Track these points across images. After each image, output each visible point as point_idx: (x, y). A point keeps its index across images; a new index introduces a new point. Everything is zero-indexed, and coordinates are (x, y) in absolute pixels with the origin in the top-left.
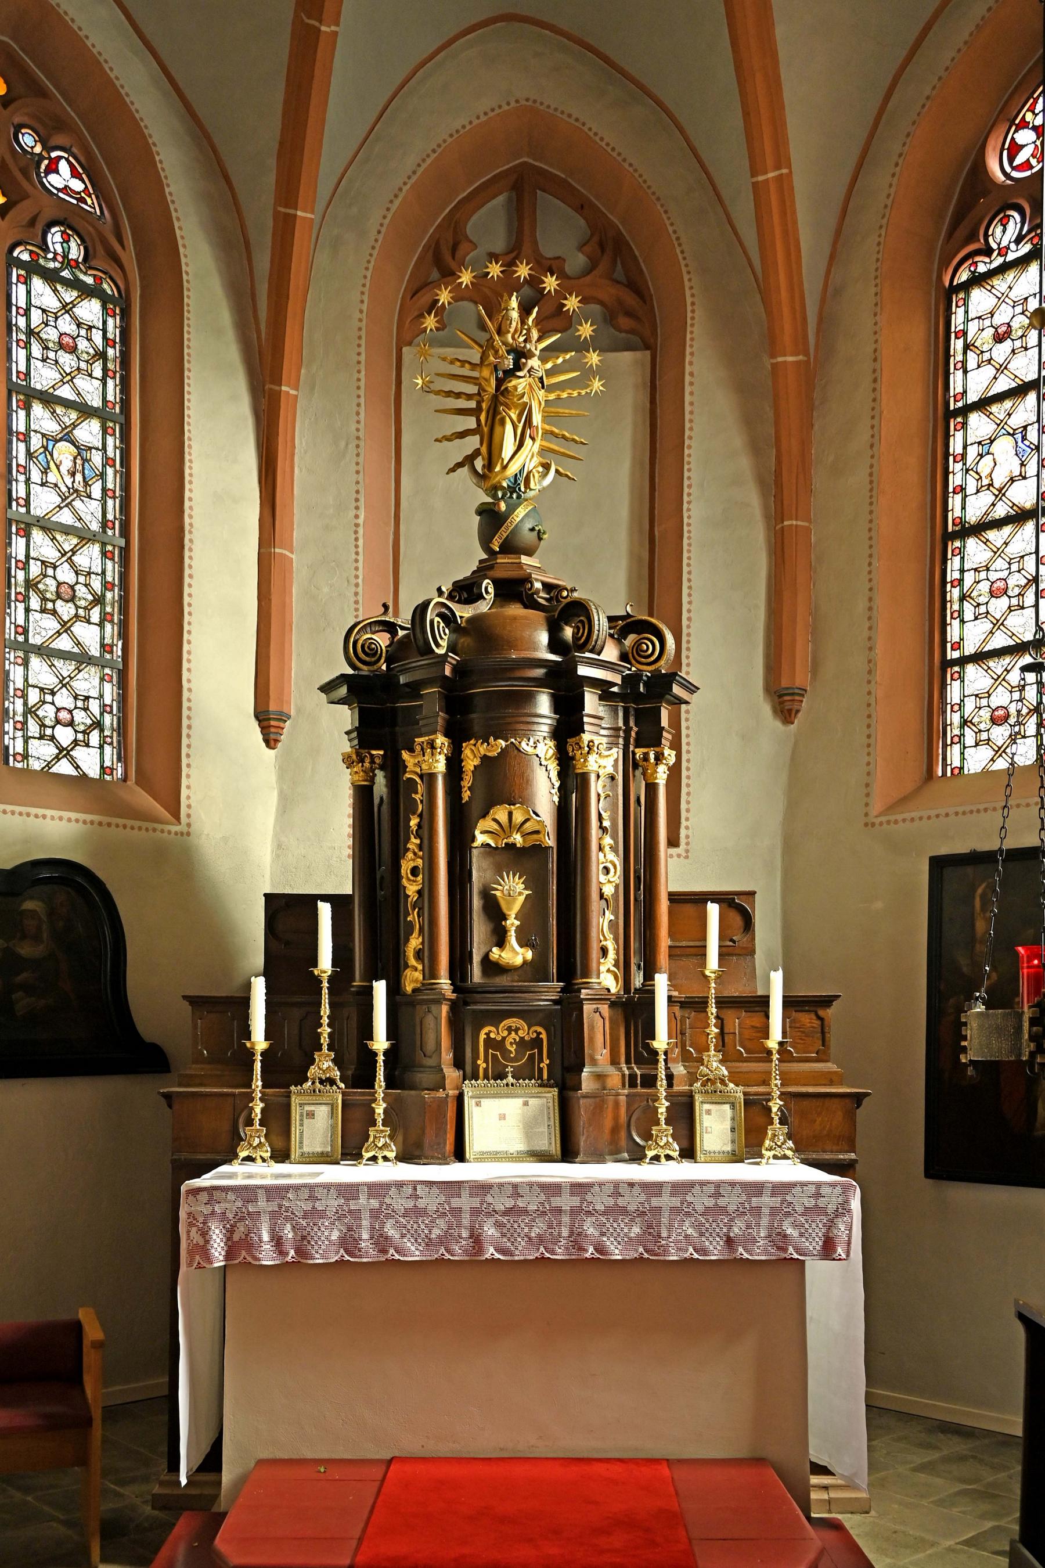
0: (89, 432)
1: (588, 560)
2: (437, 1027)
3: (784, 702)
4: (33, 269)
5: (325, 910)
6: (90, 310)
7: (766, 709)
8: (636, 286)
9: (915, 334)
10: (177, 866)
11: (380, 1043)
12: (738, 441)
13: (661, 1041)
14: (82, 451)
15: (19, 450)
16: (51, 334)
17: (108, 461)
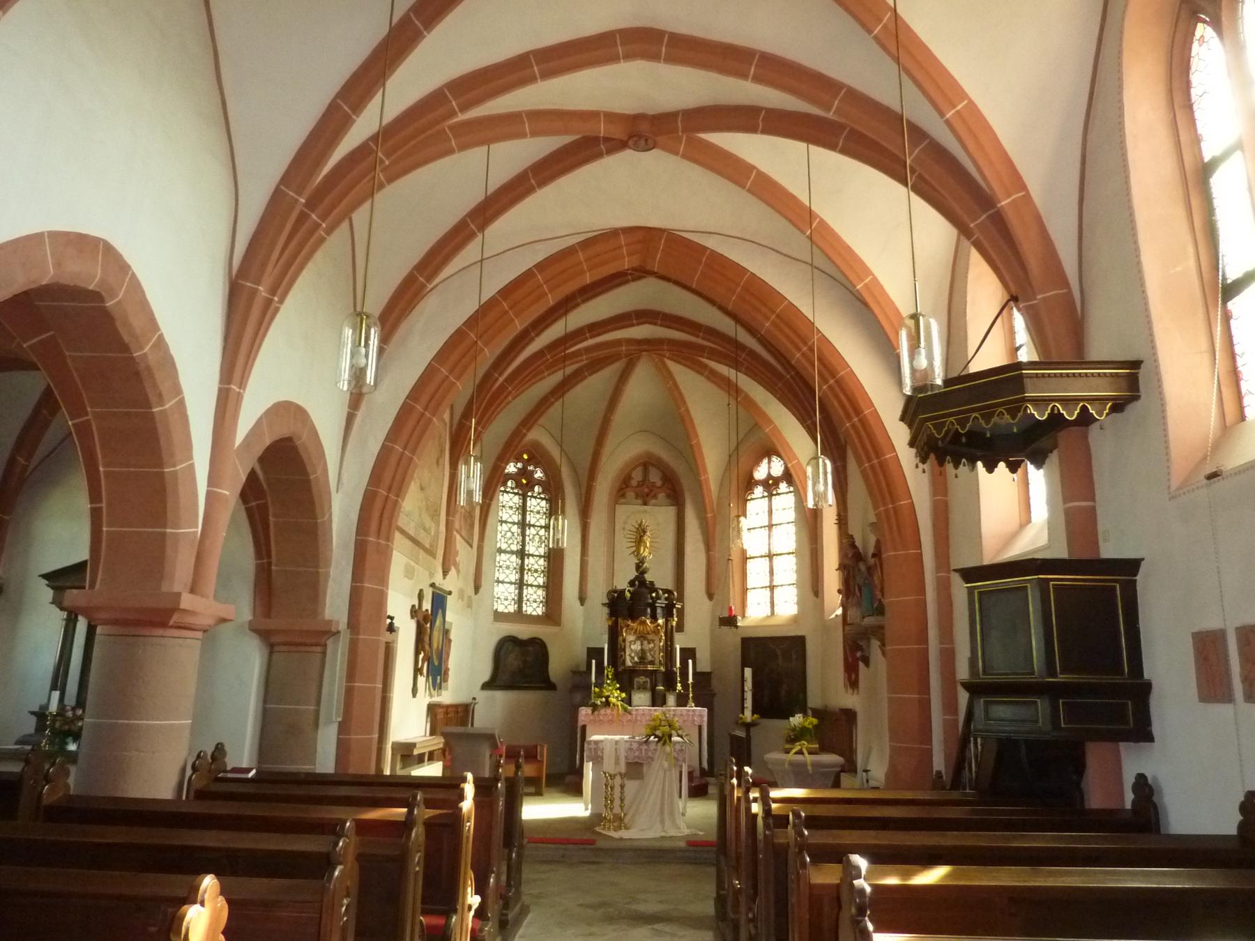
1: (660, 576)
6: (543, 503)
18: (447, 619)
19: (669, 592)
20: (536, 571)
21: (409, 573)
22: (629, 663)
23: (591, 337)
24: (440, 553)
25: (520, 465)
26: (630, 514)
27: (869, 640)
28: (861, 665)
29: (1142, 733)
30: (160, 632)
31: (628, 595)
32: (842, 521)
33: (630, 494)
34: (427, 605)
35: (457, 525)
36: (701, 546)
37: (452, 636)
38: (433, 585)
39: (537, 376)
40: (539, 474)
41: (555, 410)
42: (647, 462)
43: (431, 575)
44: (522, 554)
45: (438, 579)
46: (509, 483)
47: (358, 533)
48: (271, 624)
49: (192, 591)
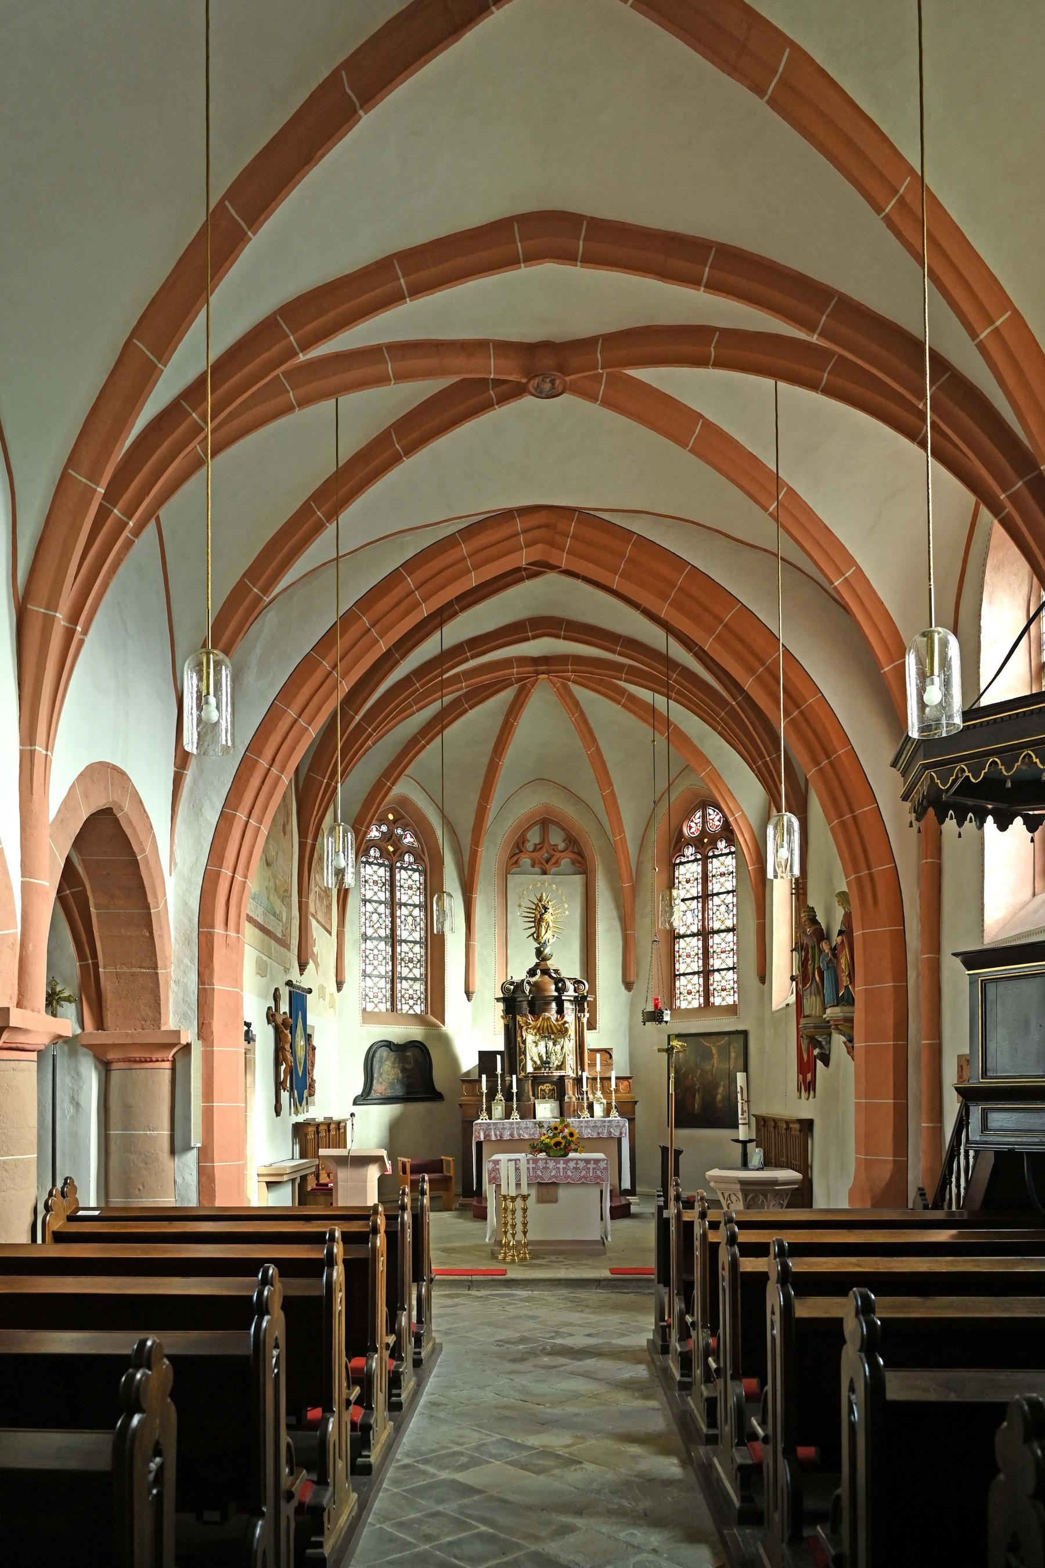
0: (416, 912)
1: (566, 963)
3: (628, 985)
4: (402, 868)
5: (499, 1057)
6: (416, 876)
7: (623, 987)
8: (580, 854)
9: (665, 877)
11: (515, 1090)
12: (612, 906)
13: (585, 1089)
14: (414, 918)
15: (398, 921)
16: (406, 885)
17: (421, 920)
18: (309, 1022)
19: (577, 982)
20: (411, 960)
21: (262, 970)
22: (530, 1069)
23: (473, 657)
24: (295, 942)
25: (384, 828)
26: (527, 885)
27: (830, 1035)
28: (819, 1063)
31: (527, 988)
32: (800, 888)
33: (526, 861)
34: (284, 1007)
35: (312, 909)
36: (617, 924)
37: (315, 1042)
38: (289, 983)
39: (404, 712)
40: (409, 839)
41: (430, 752)
42: (545, 822)
43: (287, 970)
44: (393, 940)
45: (294, 975)
46: (372, 853)
47: (200, 925)
48: (102, 1038)
49: (19, 1005)
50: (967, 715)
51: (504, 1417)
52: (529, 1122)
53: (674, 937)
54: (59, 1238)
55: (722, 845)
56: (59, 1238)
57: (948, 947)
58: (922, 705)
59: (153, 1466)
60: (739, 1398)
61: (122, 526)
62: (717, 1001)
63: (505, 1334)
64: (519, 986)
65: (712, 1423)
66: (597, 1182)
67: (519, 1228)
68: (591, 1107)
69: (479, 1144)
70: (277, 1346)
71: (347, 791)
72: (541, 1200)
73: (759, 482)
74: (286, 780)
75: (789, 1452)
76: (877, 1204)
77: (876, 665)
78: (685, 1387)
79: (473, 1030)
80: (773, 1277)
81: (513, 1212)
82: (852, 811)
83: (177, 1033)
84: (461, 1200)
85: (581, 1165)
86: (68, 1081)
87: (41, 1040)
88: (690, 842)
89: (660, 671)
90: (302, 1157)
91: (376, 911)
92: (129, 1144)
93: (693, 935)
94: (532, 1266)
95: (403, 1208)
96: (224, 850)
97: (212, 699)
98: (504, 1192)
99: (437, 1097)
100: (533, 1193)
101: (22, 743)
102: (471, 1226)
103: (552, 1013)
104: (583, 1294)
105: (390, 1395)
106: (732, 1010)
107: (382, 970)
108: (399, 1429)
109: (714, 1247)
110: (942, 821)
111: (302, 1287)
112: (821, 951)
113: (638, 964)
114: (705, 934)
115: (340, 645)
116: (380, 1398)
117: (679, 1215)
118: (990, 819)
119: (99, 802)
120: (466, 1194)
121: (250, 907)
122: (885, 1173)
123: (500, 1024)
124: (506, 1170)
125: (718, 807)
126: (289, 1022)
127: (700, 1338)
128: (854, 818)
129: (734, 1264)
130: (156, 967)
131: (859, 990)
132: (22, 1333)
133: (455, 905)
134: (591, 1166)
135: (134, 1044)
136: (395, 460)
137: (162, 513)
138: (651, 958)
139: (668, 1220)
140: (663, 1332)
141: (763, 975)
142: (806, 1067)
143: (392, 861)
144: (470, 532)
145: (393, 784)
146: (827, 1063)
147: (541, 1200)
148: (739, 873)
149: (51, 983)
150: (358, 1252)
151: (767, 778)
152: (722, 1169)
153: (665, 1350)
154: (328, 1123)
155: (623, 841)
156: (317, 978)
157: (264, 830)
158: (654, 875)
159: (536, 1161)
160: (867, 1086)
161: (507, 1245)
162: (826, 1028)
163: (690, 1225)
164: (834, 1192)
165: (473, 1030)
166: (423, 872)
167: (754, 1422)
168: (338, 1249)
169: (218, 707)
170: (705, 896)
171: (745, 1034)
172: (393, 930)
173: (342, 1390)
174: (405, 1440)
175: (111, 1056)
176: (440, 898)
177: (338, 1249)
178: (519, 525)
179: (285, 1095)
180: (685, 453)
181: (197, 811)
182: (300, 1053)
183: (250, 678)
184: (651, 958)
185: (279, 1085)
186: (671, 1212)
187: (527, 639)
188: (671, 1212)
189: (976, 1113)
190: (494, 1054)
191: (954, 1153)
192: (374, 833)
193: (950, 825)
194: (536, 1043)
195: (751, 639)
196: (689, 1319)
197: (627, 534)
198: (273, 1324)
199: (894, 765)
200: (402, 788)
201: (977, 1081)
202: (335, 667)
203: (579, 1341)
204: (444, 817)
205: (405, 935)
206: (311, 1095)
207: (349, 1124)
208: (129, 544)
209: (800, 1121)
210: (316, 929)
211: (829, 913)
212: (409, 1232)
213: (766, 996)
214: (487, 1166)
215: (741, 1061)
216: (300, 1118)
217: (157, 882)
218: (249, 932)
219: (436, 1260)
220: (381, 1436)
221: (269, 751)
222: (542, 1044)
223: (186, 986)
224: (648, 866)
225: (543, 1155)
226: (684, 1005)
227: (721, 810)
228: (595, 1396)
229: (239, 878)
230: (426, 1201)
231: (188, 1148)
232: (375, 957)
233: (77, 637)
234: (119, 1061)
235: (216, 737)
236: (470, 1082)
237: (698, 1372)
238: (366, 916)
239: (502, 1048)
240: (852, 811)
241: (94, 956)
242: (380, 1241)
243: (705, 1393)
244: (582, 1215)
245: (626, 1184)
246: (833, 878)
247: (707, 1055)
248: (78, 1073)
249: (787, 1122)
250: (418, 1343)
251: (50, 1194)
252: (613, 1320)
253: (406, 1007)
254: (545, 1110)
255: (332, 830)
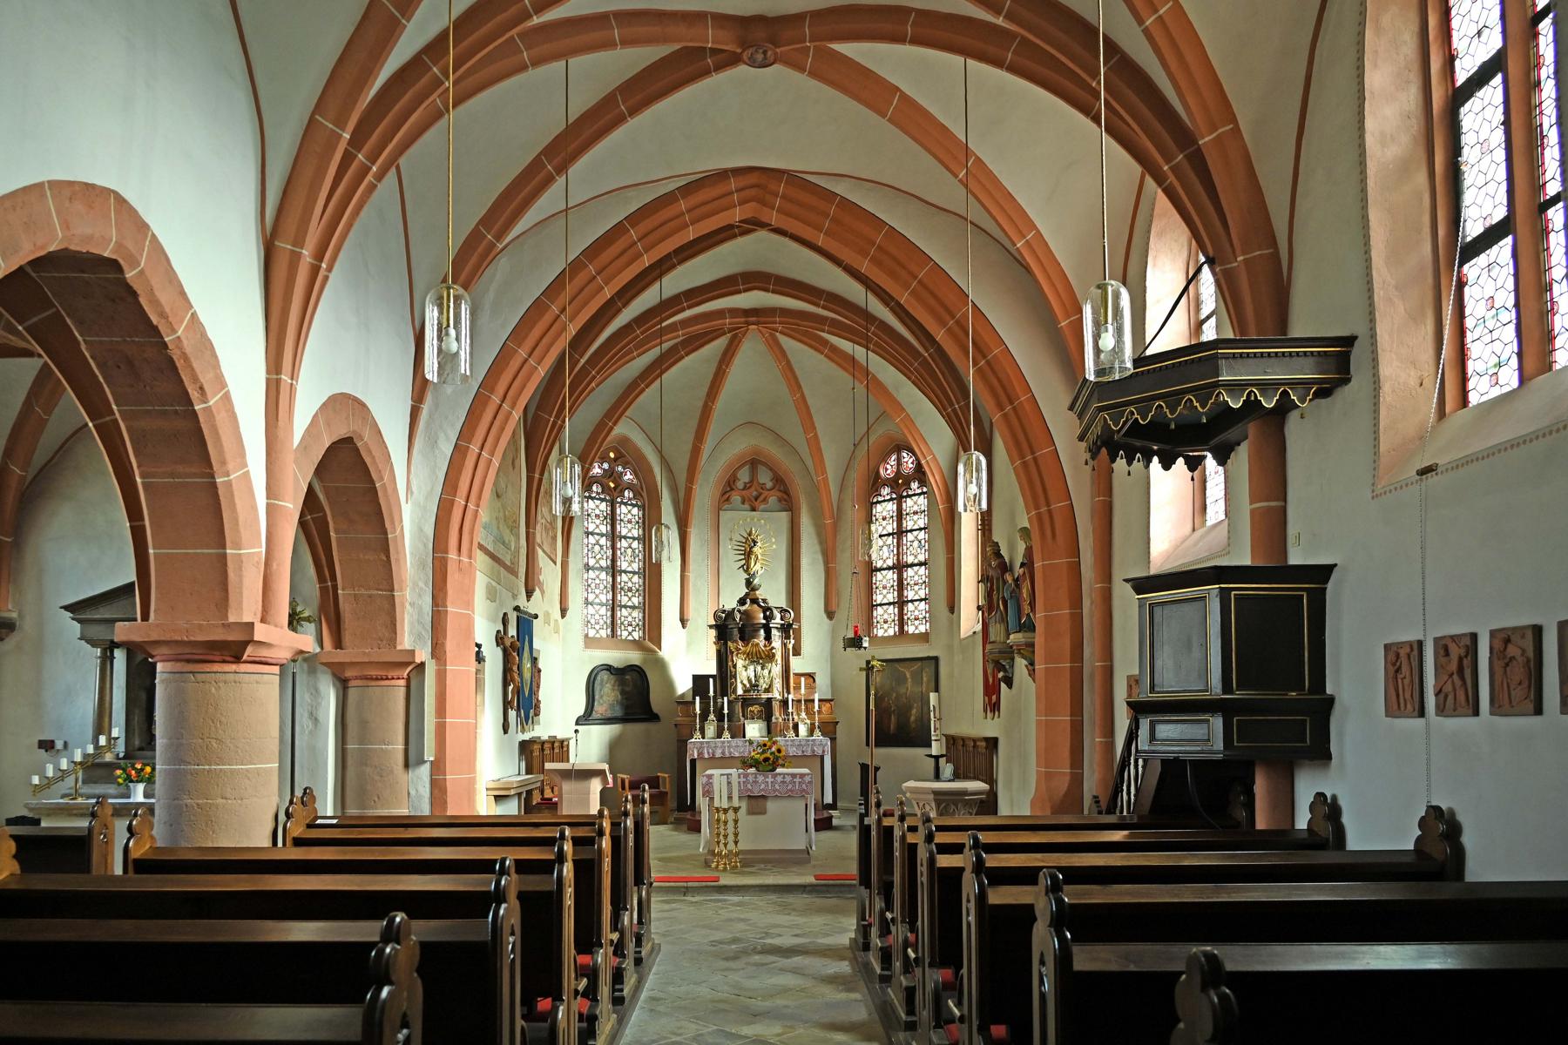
0: (635, 544)
1: (774, 593)
2: (738, 707)
3: (830, 615)
8: (786, 492)
10: (661, 665)
19: (783, 611)
20: (630, 590)
21: (492, 595)
25: (606, 466)
26: (737, 520)
29: (1320, 753)
30: (233, 667)
31: (738, 616)
32: (986, 522)
33: (736, 498)
34: (512, 631)
35: (538, 540)
36: (820, 558)
37: (540, 665)
38: (517, 609)
40: (628, 477)
43: (515, 597)
44: (614, 570)
45: (522, 601)
48: (340, 656)
49: (263, 620)
50: (1139, 361)
51: (717, 1009)
52: (739, 741)
53: (872, 570)
54: (298, 842)
55: (915, 485)
56: (298, 842)
57: (1119, 574)
58: (1098, 351)
59: (400, 1037)
60: (936, 983)
61: (365, 170)
62: (911, 629)
63: (718, 936)
64: (730, 614)
65: (911, 1011)
66: (803, 795)
67: (731, 838)
68: (796, 727)
69: (693, 762)
70: (513, 934)
71: (573, 428)
72: (751, 812)
73: (951, 152)
74: (517, 415)
75: (983, 1029)
76: (1055, 812)
77: (1054, 321)
78: (885, 980)
79: (687, 656)
80: (969, 869)
81: (726, 823)
82: (1033, 453)
83: (412, 652)
84: (676, 814)
85: (788, 779)
86: (307, 697)
87: (284, 655)
88: (886, 482)
89: (861, 325)
90: (528, 773)
91: (597, 543)
92: (365, 758)
93: (889, 568)
94: (742, 874)
95: (626, 814)
96: (458, 480)
97: (452, 332)
98: (717, 804)
99: (654, 718)
100: (744, 805)
101: (268, 372)
102: (684, 837)
103: (760, 639)
104: (791, 899)
105: (614, 990)
106: (924, 637)
107: (603, 598)
108: (621, 1021)
109: (913, 848)
110: (1113, 461)
111: (536, 883)
112: (1005, 582)
113: (838, 595)
114: (900, 567)
115: (569, 290)
116: (605, 991)
117: (879, 821)
118: (1155, 459)
119: (341, 432)
120: (681, 808)
121: (481, 536)
122: (1063, 784)
123: (713, 650)
124: (719, 786)
125: (911, 450)
126: (516, 644)
127: (899, 932)
128: (1035, 459)
129: (932, 861)
130: (392, 590)
131: (1039, 617)
132: (270, 924)
133: (671, 536)
134: (797, 780)
135: (371, 663)
136: (620, 120)
137: (402, 161)
138: (851, 589)
139: (869, 827)
140: (864, 930)
141: (953, 605)
142: (991, 690)
143: (613, 496)
144: (688, 189)
145: (615, 423)
146: (1010, 685)
147: (751, 812)
148: (930, 511)
149: (293, 603)
150: (586, 854)
151: (957, 424)
152: (915, 781)
153: (866, 947)
154: (552, 741)
155: (826, 480)
156: (543, 604)
157: (496, 463)
158: (853, 512)
159: (746, 776)
160: (1047, 705)
161: (720, 854)
162: (1009, 652)
163: (890, 830)
164: (1017, 800)
165: (687, 656)
166: (642, 508)
167: (951, 1003)
168: (568, 847)
169: (458, 339)
170: (900, 533)
171: (936, 659)
172: (614, 560)
173: (572, 982)
174: (627, 1031)
175: (349, 674)
176: (658, 530)
177: (568, 847)
178: (733, 184)
179: (512, 714)
180: (884, 121)
181: (433, 443)
182: (527, 675)
183: (484, 318)
184: (851, 589)
185: (506, 705)
186: (871, 820)
187: (739, 292)
188: (871, 820)
189: (1145, 724)
190: (707, 677)
191: (1125, 763)
192: (596, 470)
193: (1120, 464)
194: (746, 668)
195: (942, 294)
196: (889, 915)
197: (831, 196)
198: (509, 912)
199: (1071, 408)
200: (618, 430)
201: (1145, 695)
202: (563, 310)
203: (787, 941)
204: (660, 452)
205: (624, 566)
206: (537, 714)
207: (572, 743)
208: (372, 188)
209: (987, 739)
210: (542, 559)
211: (1012, 547)
212: (631, 837)
213: (955, 624)
214: (700, 781)
215: (933, 685)
216: (527, 736)
217: (395, 509)
218: (481, 559)
219: (656, 870)
220: (605, 1027)
221: (501, 388)
222: (751, 668)
223: (421, 608)
224: (848, 504)
225: (753, 770)
226: (880, 633)
227: (914, 454)
228: (802, 990)
229: (471, 506)
230: (646, 809)
231: (422, 762)
232: (597, 586)
233: (322, 273)
234: (356, 678)
235: (456, 366)
236: (685, 703)
237: (897, 965)
238: (589, 547)
239: (714, 671)
240: (1033, 453)
241: (333, 578)
242: (606, 843)
243: (905, 983)
244: (788, 826)
245: (828, 799)
246: (1016, 515)
247: (901, 680)
248: (317, 690)
249: (975, 741)
250: (639, 943)
251: (291, 802)
252: (817, 921)
253: (625, 634)
254: (754, 730)
255: (560, 462)
